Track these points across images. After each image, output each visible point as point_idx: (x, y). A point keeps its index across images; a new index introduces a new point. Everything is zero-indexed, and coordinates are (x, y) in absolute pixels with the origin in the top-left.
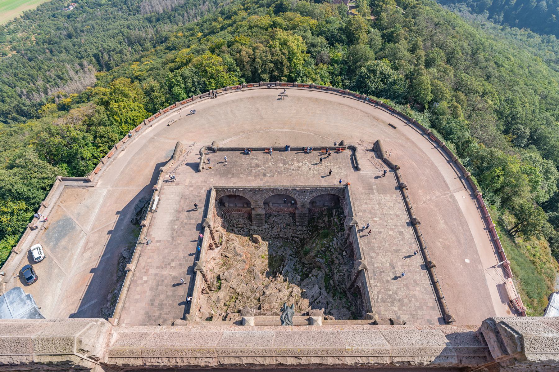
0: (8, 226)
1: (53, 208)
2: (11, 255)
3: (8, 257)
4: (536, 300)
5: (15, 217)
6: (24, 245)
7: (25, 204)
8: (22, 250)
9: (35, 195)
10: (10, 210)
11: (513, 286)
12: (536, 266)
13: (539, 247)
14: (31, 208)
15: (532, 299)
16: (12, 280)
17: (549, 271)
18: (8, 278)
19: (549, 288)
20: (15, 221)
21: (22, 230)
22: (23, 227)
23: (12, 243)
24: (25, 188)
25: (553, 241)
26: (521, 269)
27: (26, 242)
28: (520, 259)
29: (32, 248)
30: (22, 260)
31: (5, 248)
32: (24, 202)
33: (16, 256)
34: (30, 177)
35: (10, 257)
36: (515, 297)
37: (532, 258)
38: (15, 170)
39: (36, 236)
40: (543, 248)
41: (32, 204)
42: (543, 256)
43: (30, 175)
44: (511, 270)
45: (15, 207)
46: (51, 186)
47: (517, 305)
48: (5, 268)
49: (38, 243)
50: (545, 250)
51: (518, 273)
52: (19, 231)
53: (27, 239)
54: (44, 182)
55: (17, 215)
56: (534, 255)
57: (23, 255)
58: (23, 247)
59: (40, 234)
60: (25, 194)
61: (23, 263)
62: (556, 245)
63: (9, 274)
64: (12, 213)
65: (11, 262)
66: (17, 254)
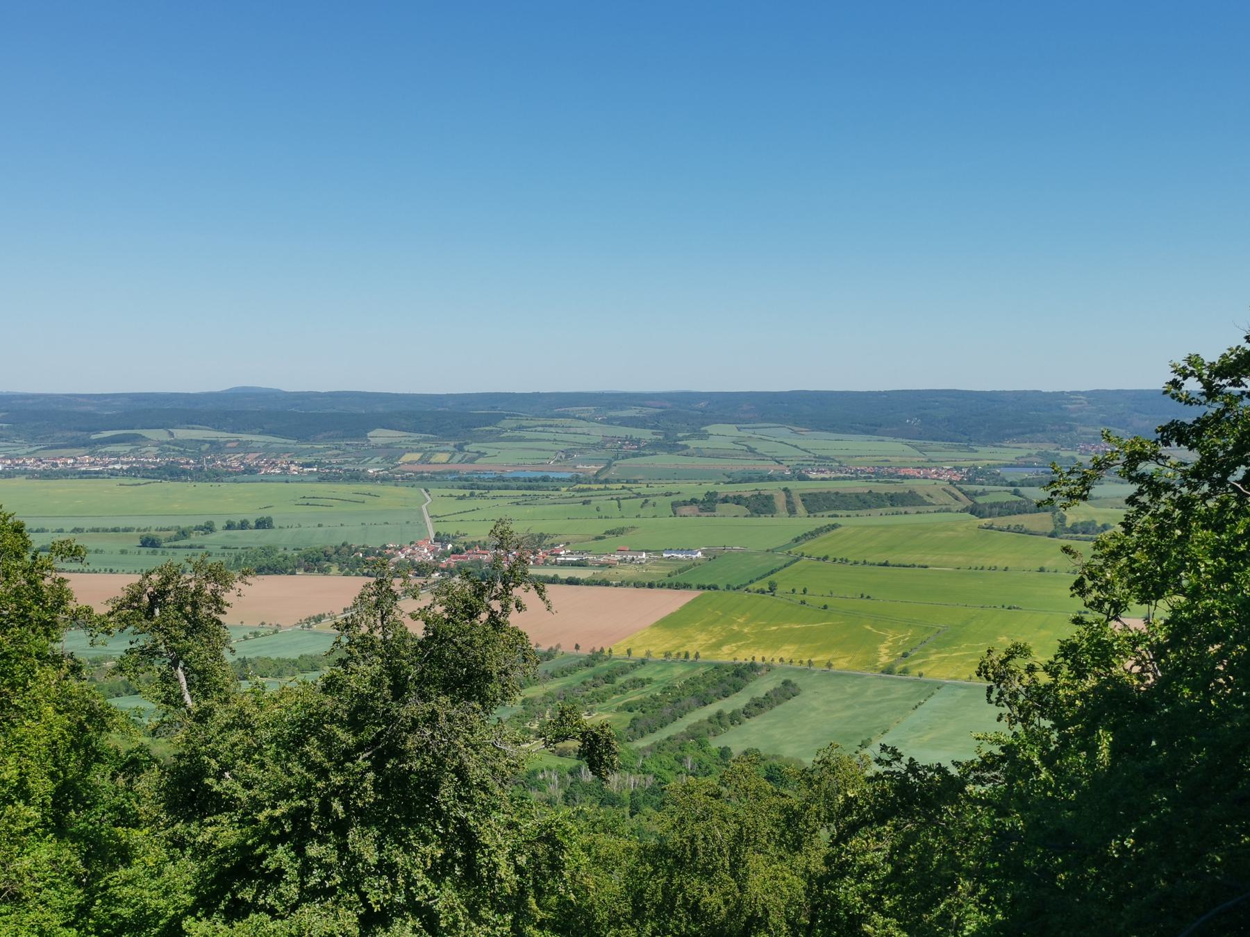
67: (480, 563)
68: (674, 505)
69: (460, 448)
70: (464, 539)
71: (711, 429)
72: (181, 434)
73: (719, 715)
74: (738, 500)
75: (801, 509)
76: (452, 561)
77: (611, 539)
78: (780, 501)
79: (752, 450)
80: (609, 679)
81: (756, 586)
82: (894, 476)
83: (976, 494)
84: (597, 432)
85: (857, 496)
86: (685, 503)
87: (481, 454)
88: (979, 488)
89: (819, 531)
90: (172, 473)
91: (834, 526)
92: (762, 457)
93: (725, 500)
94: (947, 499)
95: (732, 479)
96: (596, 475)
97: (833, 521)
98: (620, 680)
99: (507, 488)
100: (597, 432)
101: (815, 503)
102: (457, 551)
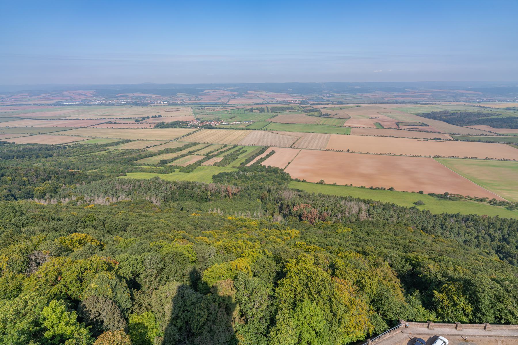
0: (441, 308)
1: (489, 336)
2: (425, 323)
3: (419, 322)
5: (454, 309)
6: (439, 329)
7: (472, 310)
8: (433, 329)
9: (487, 313)
10: (457, 302)
14: (471, 317)
16: (405, 335)
18: (406, 331)
20: (450, 311)
21: (446, 320)
22: (450, 319)
23: (431, 319)
24: (487, 303)
27: (442, 329)
29: (441, 337)
30: (425, 334)
31: (424, 315)
32: (472, 309)
33: (426, 327)
34: (503, 300)
35: (422, 324)
38: (498, 285)
39: (453, 335)
41: (476, 316)
43: (505, 299)
45: (462, 304)
46: (508, 323)
48: (412, 324)
49: (449, 340)
52: (444, 318)
53: (445, 329)
54: (507, 314)
55: (456, 310)
57: (429, 333)
58: (436, 329)
59: (457, 337)
60: (482, 305)
61: (424, 336)
63: (409, 331)
64: (455, 305)
65: (419, 326)
66: (428, 327)
67: (207, 125)
68: (244, 110)
69: (197, 97)
70: (202, 119)
71: (249, 92)
72: (136, 94)
73: (262, 158)
74: (257, 109)
75: (270, 111)
76: (202, 124)
77: (233, 119)
78: (266, 109)
79: (258, 97)
80: (239, 150)
81: (263, 129)
82: (287, 103)
83: (304, 107)
84: (226, 93)
85: (281, 108)
86: (247, 110)
87: (201, 98)
88: (305, 106)
89: (274, 116)
90: (136, 104)
91: (277, 115)
92: (260, 98)
93: (255, 109)
94: (298, 108)
95: (256, 104)
96: (227, 103)
97: (277, 114)
98: (241, 151)
99: (209, 106)
100: (226, 93)
101: (273, 110)
102: (202, 122)
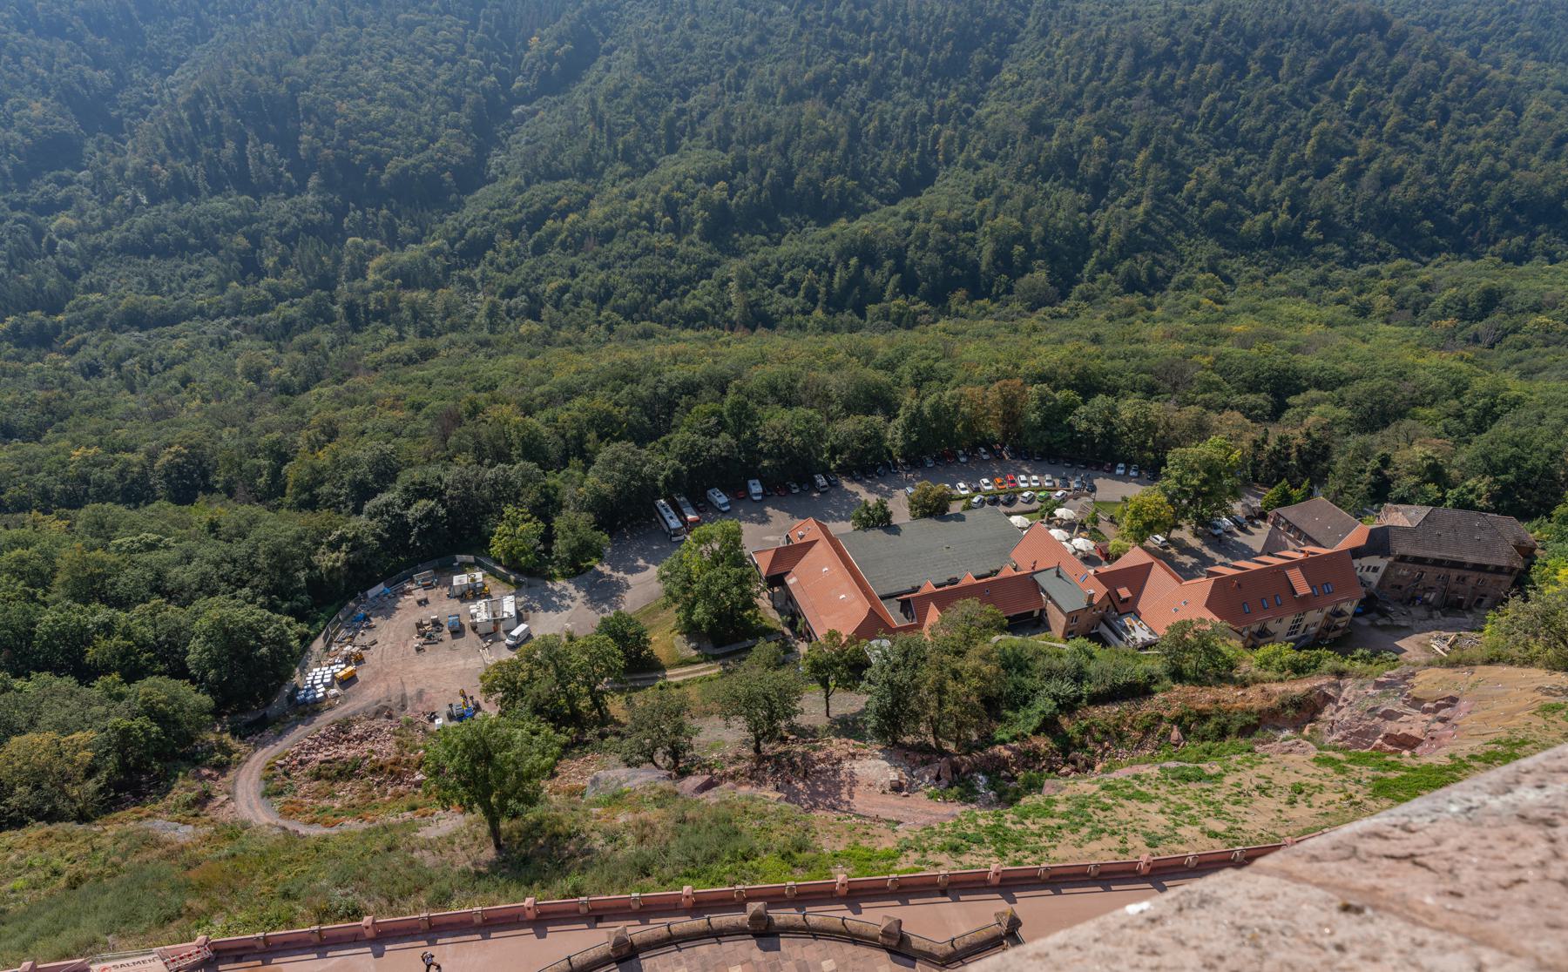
4: (189, 902)
11: (118, 963)
12: (90, 875)
13: (36, 853)
15: (183, 911)
17: (124, 844)
19: (170, 855)
25: (47, 808)
26: (77, 925)
28: (40, 922)
36: (160, 963)
37: (62, 882)
40: (47, 842)
42: (68, 849)
44: (61, 958)
47: (190, 961)
50: (52, 840)
51: (83, 935)
56: (56, 873)
62: (61, 804)
